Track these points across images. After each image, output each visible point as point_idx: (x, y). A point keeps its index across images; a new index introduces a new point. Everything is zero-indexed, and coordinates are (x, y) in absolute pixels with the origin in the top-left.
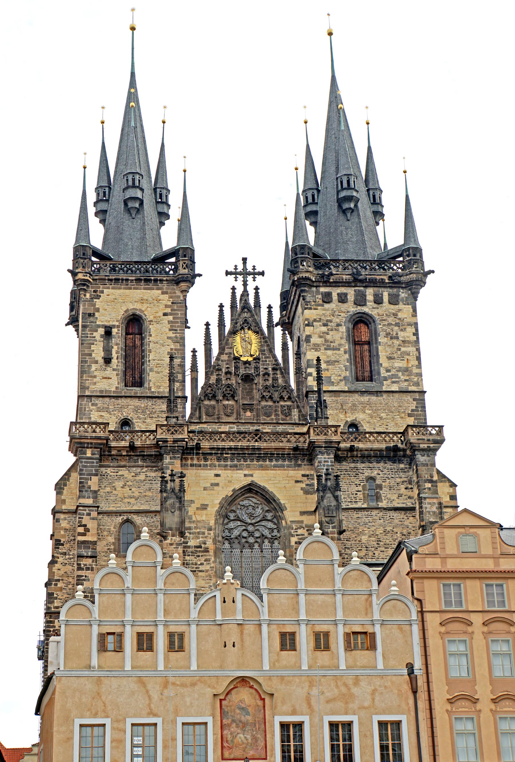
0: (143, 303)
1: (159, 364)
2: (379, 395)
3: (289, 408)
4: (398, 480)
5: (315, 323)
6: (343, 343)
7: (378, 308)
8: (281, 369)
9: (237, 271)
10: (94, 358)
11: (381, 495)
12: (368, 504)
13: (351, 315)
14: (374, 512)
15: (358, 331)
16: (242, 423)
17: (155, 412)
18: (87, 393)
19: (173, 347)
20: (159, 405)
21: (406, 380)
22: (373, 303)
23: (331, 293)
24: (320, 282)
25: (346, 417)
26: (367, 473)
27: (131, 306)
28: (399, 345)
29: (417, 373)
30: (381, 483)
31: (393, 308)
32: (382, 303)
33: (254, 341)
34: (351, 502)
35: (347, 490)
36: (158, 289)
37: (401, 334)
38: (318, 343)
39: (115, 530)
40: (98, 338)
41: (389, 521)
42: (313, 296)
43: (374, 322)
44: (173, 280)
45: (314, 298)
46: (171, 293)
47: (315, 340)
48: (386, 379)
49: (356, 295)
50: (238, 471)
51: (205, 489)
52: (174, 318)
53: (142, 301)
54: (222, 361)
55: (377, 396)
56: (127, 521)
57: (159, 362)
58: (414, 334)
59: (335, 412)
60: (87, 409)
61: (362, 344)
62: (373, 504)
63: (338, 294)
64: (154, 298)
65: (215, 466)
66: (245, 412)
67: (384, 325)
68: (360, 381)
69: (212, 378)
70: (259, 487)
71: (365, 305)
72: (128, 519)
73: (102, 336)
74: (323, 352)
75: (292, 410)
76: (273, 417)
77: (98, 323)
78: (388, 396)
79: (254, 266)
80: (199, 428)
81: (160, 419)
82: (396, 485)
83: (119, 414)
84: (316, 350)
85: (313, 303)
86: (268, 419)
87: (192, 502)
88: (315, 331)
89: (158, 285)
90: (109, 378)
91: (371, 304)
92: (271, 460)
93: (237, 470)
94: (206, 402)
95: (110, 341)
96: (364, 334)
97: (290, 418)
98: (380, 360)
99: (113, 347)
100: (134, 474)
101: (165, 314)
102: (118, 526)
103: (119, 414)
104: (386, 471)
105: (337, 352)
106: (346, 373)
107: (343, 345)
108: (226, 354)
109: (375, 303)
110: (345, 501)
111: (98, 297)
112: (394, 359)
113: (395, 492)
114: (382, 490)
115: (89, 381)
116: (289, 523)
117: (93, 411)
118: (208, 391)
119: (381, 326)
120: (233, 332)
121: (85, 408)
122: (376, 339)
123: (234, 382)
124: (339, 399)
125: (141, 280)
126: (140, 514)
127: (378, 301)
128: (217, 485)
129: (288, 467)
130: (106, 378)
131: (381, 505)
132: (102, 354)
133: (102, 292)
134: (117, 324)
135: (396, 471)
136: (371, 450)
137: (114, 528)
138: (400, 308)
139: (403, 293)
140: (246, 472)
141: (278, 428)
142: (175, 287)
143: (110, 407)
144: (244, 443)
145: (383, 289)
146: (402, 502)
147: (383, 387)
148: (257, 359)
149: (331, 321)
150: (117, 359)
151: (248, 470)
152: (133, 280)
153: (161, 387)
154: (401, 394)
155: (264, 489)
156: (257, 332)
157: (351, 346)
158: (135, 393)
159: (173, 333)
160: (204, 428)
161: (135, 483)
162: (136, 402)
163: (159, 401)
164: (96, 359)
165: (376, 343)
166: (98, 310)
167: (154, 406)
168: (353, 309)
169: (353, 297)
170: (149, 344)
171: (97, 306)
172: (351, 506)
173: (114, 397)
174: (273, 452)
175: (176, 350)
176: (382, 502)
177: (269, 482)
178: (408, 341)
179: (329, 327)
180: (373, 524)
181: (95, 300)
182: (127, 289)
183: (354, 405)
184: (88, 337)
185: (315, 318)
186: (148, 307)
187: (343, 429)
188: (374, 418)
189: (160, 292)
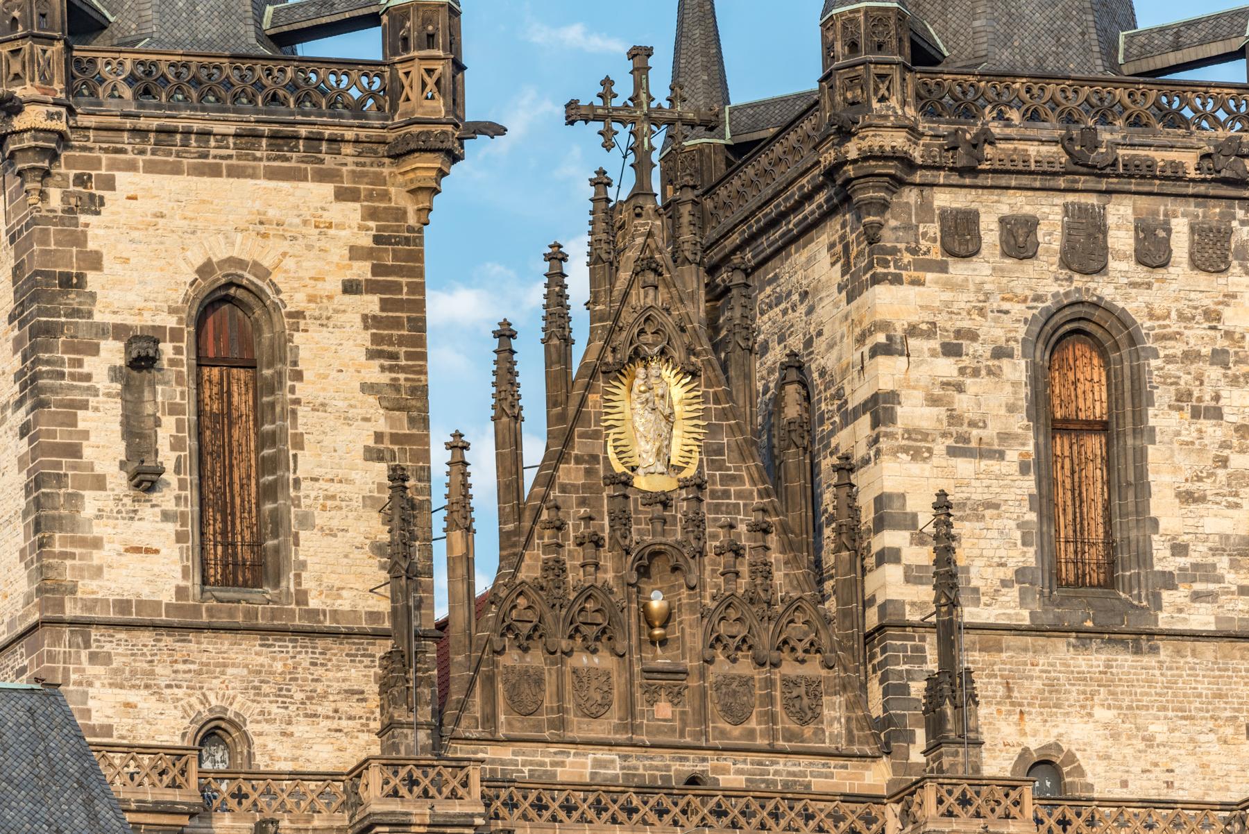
0: (265, 236)
1: (333, 497)
3: (814, 690)
5: (912, 342)
7: (1149, 286)
9: (616, 103)
13: (1048, 308)
17: (325, 695)
18: (71, 610)
19: (382, 426)
20: (339, 669)
23: (976, 214)
25: (1024, 734)
27: (220, 253)
28: (1225, 445)
31: (1206, 288)
36: (323, 176)
38: (925, 425)
40: (102, 381)
42: (907, 227)
46: (370, 197)
47: (913, 412)
48: (1169, 581)
49: (1069, 231)
52: (385, 305)
53: (262, 226)
55: (1138, 651)
57: (334, 488)
60: (74, 677)
63: (1003, 221)
66: (652, 703)
67: (1169, 359)
69: (527, 561)
71: (1102, 270)
76: (753, 723)
77: (98, 318)
78: (1178, 652)
81: (344, 723)
83: (194, 700)
84: (916, 455)
85: (907, 258)
86: (737, 731)
88: (914, 374)
89: (322, 161)
90: (148, 551)
91: (1123, 266)
94: (511, 658)
95: (147, 395)
97: (815, 734)
98: (1153, 502)
99: (158, 423)
101: (351, 288)
103: (194, 700)
106: (1024, 554)
107: (1016, 436)
109: (1140, 262)
111: (94, 205)
112: (1202, 499)
115: (77, 562)
117: (97, 684)
120: (612, 368)
122: (1139, 417)
123: (610, 576)
124: (996, 657)
127: (1152, 252)
130: (137, 550)
132: (119, 449)
133: (109, 184)
134: (171, 322)
138: (1232, 289)
143: (159, 670)
147: (1161, 615)
149: (973, 336)
150: (177, 470)
153: (344, 593)
154: (1226, 645)
157: (1041, 439)
158: (250, 614)
159: (383, 369)
160: (502, 762)
162: (248, 654)
163: (338, 651)
164: (98, 470)
165: (1137, 432)
166: (95, 261)
167: (319, 671)
168: (1055, 288)
170: (294, 412)
171: (91, 246)
173: (169, 628)
175: (395, 438)
179: (966, 361)
181: (83, 218)
182: (202, 174)
183: (1053, 686)
184: (61, 375)
185: (914, 319)
186: (284, 254)
188: (1123, 739)
189: (328, 189)
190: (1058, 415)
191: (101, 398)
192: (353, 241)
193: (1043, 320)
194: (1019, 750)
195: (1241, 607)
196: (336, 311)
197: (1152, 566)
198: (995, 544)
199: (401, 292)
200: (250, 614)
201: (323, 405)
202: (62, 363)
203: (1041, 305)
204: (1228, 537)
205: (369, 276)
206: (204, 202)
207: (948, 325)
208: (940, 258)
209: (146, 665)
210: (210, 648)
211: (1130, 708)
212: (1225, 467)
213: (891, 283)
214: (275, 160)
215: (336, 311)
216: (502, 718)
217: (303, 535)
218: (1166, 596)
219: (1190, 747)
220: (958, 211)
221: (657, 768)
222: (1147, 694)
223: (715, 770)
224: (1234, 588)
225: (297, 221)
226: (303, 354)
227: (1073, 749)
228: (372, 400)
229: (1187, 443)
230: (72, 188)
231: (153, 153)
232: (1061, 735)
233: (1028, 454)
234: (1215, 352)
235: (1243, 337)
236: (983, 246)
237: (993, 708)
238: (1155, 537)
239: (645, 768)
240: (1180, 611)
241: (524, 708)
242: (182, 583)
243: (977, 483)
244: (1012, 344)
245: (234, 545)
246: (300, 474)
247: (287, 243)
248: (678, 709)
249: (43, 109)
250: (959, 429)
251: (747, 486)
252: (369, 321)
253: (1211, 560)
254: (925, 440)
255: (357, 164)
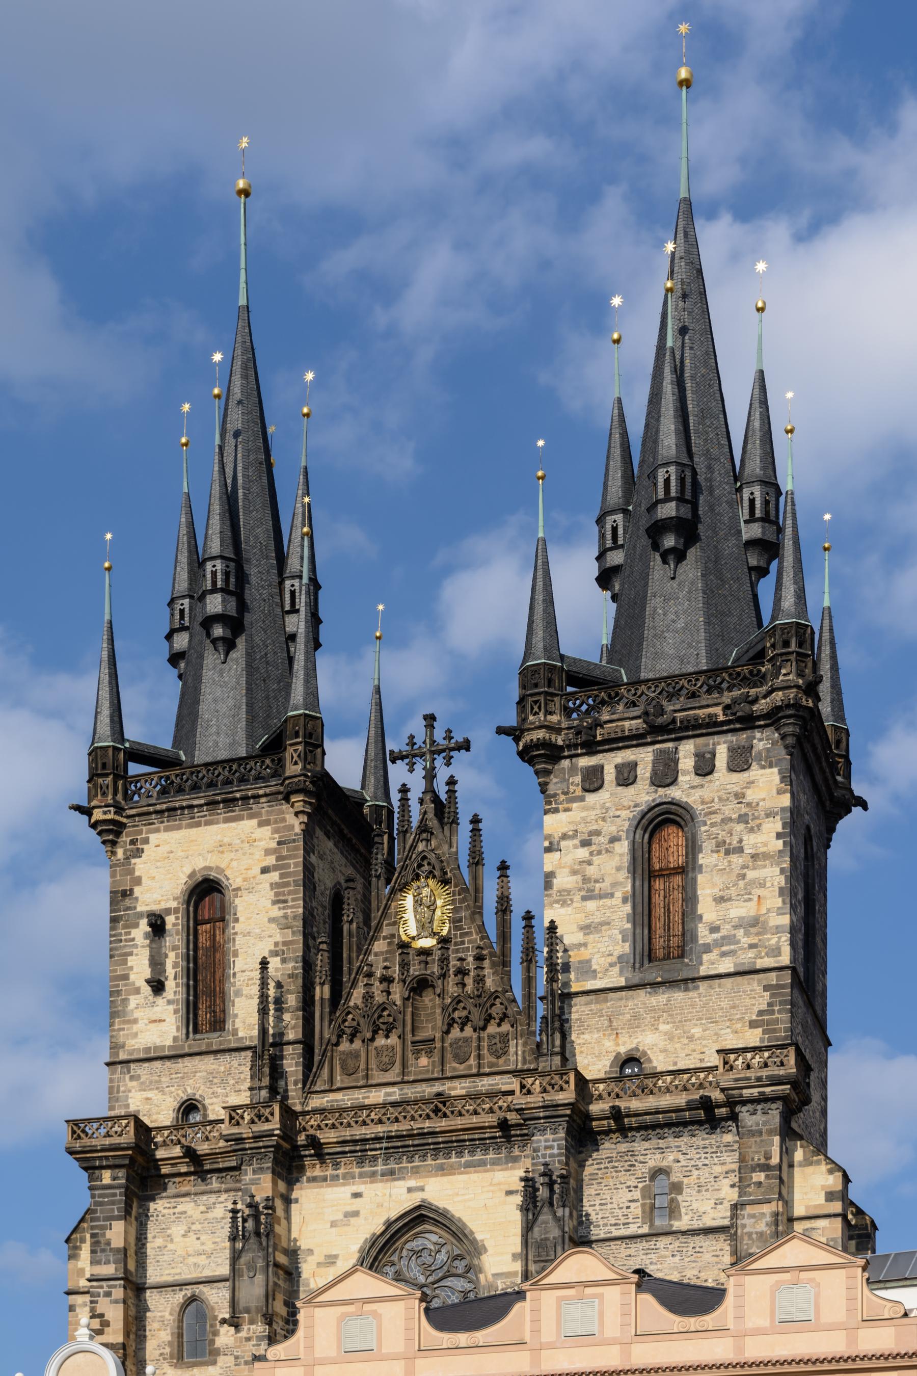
0: (222, 852)
1: (252, 979)
2: (690, 985)
4: (718, 1169)
6: (621, 880)
7: (702, 786)
8: (492, 954)
10: (134, 983)
11: (678, 1206)
12: (652, 1225)
13: (642, 810)
14: (663, 1242)
15: (661, 846)
16: (408, 1082)
18: (123, 1056)
19: (278, 938)
21: (752, 946)
22: (693, 775)
23: (602, 767)
24: (576, 746)
25: (618, 1045)
26: (654, 1160)
28: (744, 867)
29: (777, 927)
30: (681, 1178)
32: (711, 772)
33: (439, 903)
34: (615, 1225)
35: (609, 1200)
36: (251, 817)
37: (751, 842)
38: (569, 886)
39: (172, 1318)
41: (692, 1258)
43: (693, 820)
44: (279, 793)
45: (564, 785)
46: (276, 822)
47: (563, 881)
50: (396, 1183)
51: (333, 1224)
52: (282, 876)
54: (376, 955)
56: (193, 1299)
58: (779, 836)
59: (596, 1036)
60: (122, 1089)
61: (669, 875)
62: (660, 1223)
64: (243, 837)
65: (354, 1178)
67: (713, 825)
68: (660, 960)
69: (355, 994)
70: (436, 1211)
71: (674, 782)
72: (194, 1295)
73: (147, 935)
74: (579, 905)
75: (511, 1042)
76: (472, 1061)
77: (139, 909)
78: (711, 987)
79: (449, 731)
80: (328, 1102)
82: (712, 1180)
84: (564, 903)
85: (562, 797)
86: (462, 1066)
87: (310, 1251)
88: (564, 860)
89: (251, 809)
90: (160, 1021)
91: (687, 778)
92: (460, 1154)
93: (395, 1180)
96: (672, 846)
99: (166, 956)
100: (203, 1208)
101: (265, 870)
102: (178, 1309)
104: (692, 1153)
105: (608, 902)
108: (385, 938)
109: (697, 774)
110: (605, 1225)
111: (139, 853)
112: (730, 899)
113: (708, 1195)
114: (681, 1194)
116: (490, 1278)
117: (133, 1091)
118: (347, 1024)
119: (706, 828)
121: (119, 1086)
124: (604, 1006)
125: (218, 803)
126: (216, 1284)
127: (705, 768)
128: (356, 1214)
129: (493, 1164)
130: (155, 1021)
131: (677, 1225)
132: (147, 973)
133: (146, 841)
134: (174, 904)
135: (714, 1150)
136: (658, 1112)
137: (171, 1314)
138: (752, 779)
139: (760, 740)
140: (412, 1183)
141: (480, 1084)
142: (284, 807)
143: (163, 1079)
144: (404, 1127)
145: (716, 738)
146: (721, 1215)
147: (702, 968)
148: (444, 941)
149: (598, 833)
150: (175, 978)
151: (415, 1179)
152: (201, 806)
154: (739, 979)
155: (444, 1214)
156: (445, 882)
159: (280, 909)
160: (337, 1101)
161: (206, 1225)
162: (208, 1064)
164: (137, 984)
165: (694, 869)
166: (138, 881)
167: (243, 1068)
169: (649, 768)
170: (234, 939)
171: (137, 874)
172: (616, 1233)
174: (462, 1137)
175: (285, 943)
176: (679, 1218)
177: (456, 1199)
178: (763, 853)
179: (594, 848)
180: (659, 1266)
181: (133, 861)
183: (636, 1016)
184: (121, 941)
185: (565, 830)
186: (232, 860)
187: (610, 1072)
188: (676, 1040)
189: (254, 822)
190: (657, 868)
191: (139, 949)
192: (267, 846)
193: (639, 817)
194: (614, 1054)
195: (750, 955)
196: (257, 884)
197: (697, 941)
198: (606, 944)
199: (290, 867)
200: (208, 1045)
201: (249, 933)
202: (121, 934)
203: (638, 809)
204: (743, 918)
205: (274, 862)
206: (192, 841)
207: (584, 830)
208: (581, 794)
209: (157, 1078)
210: (189, 1064)
211: (680, 1021)
212: (744, 879)
213: (553, 813)
214: (228, 812)
215: (257, 884)
216: (339, 1078)
217: (236, 1000)
218: (705, 957)
219: (715, 1038)
220: (589, 767)
221: (418, 1092)
222: (691, 1013)
223: (449, 1089)
224: (746, 946)
225: (239, 841)
226: (239, 909)
227: (646, 1049)
228: (274, 926)
229: (721, 870)
230: (128, 847)
231: (168, 821)
232: (639, 1042)
233: (627, 892)
234: (740, 816)
235: (758, 804)
236: (606, 782)
237: (601, 1034)
238: (700, 925)
239: (412, 1093)
240: (713, 964)
241: (349, 1072)
242: (176, 1034)
243: (596, 913)
244: (621, 833)
245: (214, 1012)
246: (236, 970)
247: (233, 854)
248: (432, 1059)
249: (101, 810)
250: (589, 885)
251: (474, 936)
252: (273, 886)
253: (733, 932)
254: (569, 895)
255: (269, 806)
